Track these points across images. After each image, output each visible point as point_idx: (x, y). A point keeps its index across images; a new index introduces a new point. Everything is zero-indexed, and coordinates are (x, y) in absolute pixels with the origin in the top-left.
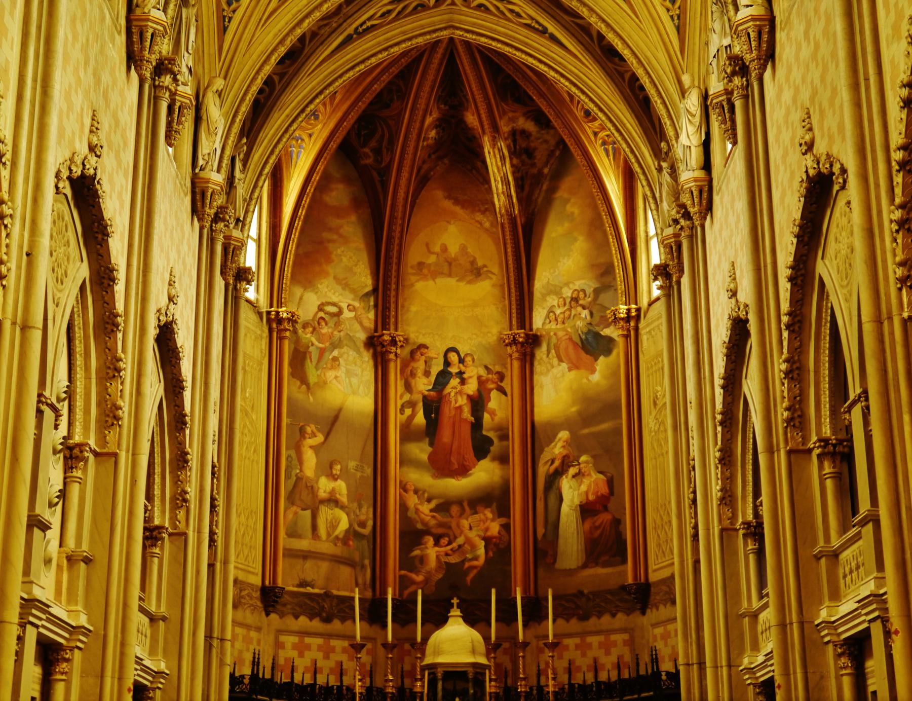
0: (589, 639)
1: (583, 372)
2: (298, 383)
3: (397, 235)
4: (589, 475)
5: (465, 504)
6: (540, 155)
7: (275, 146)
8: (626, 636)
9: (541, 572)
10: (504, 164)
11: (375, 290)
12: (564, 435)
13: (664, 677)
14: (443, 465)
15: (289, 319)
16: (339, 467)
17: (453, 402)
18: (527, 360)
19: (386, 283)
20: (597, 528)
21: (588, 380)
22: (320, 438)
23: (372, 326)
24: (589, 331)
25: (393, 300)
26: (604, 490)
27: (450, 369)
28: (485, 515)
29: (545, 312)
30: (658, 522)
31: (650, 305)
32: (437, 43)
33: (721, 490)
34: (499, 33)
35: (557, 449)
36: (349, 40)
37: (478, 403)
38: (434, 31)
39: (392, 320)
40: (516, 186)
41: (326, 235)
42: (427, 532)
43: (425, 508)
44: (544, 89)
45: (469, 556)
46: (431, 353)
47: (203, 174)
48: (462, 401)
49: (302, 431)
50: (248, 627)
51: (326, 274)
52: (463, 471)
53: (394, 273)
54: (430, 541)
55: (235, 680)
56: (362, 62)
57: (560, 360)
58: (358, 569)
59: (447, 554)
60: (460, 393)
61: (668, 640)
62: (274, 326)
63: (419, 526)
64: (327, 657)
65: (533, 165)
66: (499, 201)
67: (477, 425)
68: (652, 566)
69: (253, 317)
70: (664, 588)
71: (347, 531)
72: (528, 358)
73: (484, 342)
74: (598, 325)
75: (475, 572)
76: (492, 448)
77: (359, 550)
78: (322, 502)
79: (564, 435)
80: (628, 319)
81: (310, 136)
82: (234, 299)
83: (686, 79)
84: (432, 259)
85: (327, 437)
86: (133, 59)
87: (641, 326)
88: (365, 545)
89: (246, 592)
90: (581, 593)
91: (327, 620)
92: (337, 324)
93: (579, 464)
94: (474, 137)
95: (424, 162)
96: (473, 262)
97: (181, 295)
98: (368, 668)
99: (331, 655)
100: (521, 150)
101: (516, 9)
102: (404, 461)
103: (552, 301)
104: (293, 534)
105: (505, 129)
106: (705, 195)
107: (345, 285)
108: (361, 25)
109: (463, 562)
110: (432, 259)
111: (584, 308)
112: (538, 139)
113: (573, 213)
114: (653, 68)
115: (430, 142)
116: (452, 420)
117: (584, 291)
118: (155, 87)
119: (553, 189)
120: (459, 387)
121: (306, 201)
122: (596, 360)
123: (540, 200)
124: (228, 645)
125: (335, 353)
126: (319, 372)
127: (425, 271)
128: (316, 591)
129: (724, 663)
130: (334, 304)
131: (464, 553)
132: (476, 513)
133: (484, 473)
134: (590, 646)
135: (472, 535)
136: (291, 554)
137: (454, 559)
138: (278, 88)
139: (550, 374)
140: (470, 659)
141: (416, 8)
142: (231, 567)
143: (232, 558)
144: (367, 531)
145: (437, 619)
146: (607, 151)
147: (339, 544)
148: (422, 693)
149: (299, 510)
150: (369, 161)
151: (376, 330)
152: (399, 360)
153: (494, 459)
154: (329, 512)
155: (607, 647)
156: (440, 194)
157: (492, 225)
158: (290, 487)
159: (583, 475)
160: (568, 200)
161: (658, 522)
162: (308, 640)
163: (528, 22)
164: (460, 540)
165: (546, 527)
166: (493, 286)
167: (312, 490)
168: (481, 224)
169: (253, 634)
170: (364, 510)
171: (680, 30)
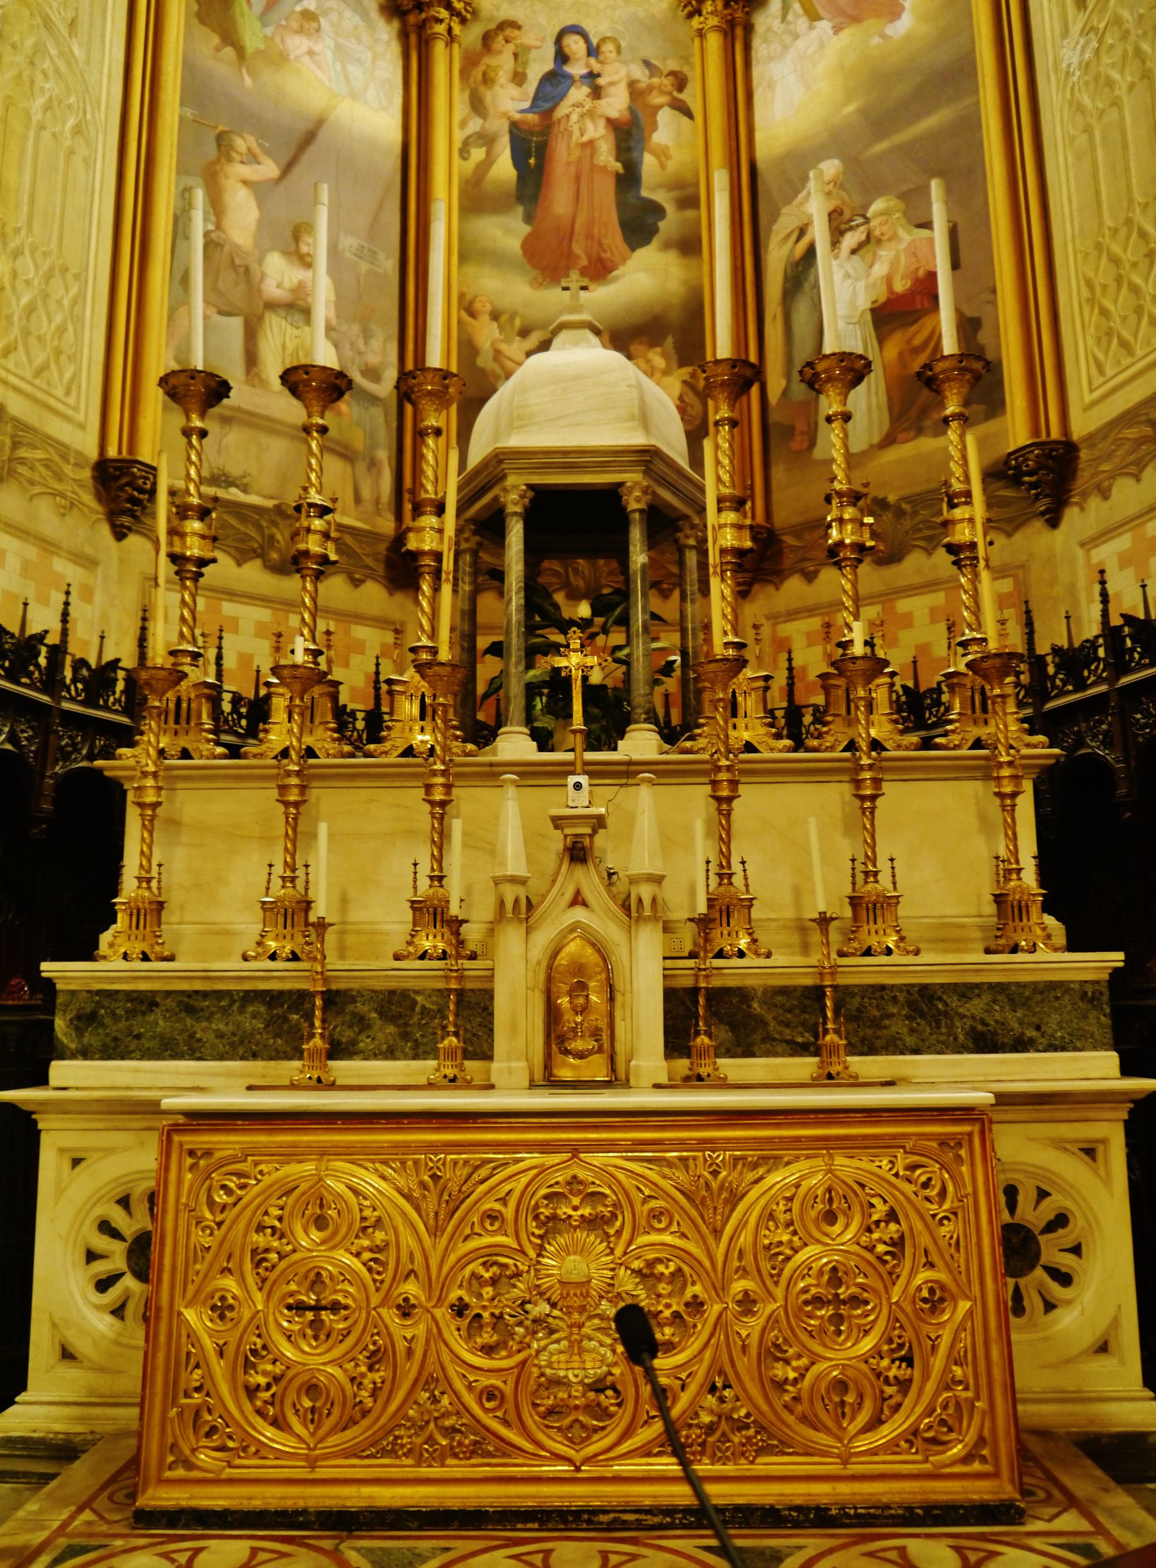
0: (904, 605)
1: (870, 24)
2: (216, 40)
4: (894, 237)
9: (779, 473)
12: (831, 167)
17: (576, 134)
20: (916, 351)
21: (883, 36)
22: (269, 169)
28: (648, 361)
37: (629, 135)
46: (527, 37)
48: (597, 131)
49: (222, 140)
52: (600, 270)
57: (813, 16)
58: (361, 466)
60: (591, 114)
67: (629, 178)
68: (1074, 411)
70: (1131, 433)
72: (739, 32)
73: (641, 14)
76: (662, 225)
78: (271, 306)
89: (39, 454)
93: (867, 220)
116: (573, 170)
120: (588, 104)
126: (269, 31)
128: (254, 499)
139: (791, 54)
140: (638, 439)
148: (438, 556)
152: (456, 47)
153: (667, 246)
154: (291, 331)
159: (879, 242)
161: (1104, 274)
165: (788, 376)
167: (247, 275)
170: (376, 343)
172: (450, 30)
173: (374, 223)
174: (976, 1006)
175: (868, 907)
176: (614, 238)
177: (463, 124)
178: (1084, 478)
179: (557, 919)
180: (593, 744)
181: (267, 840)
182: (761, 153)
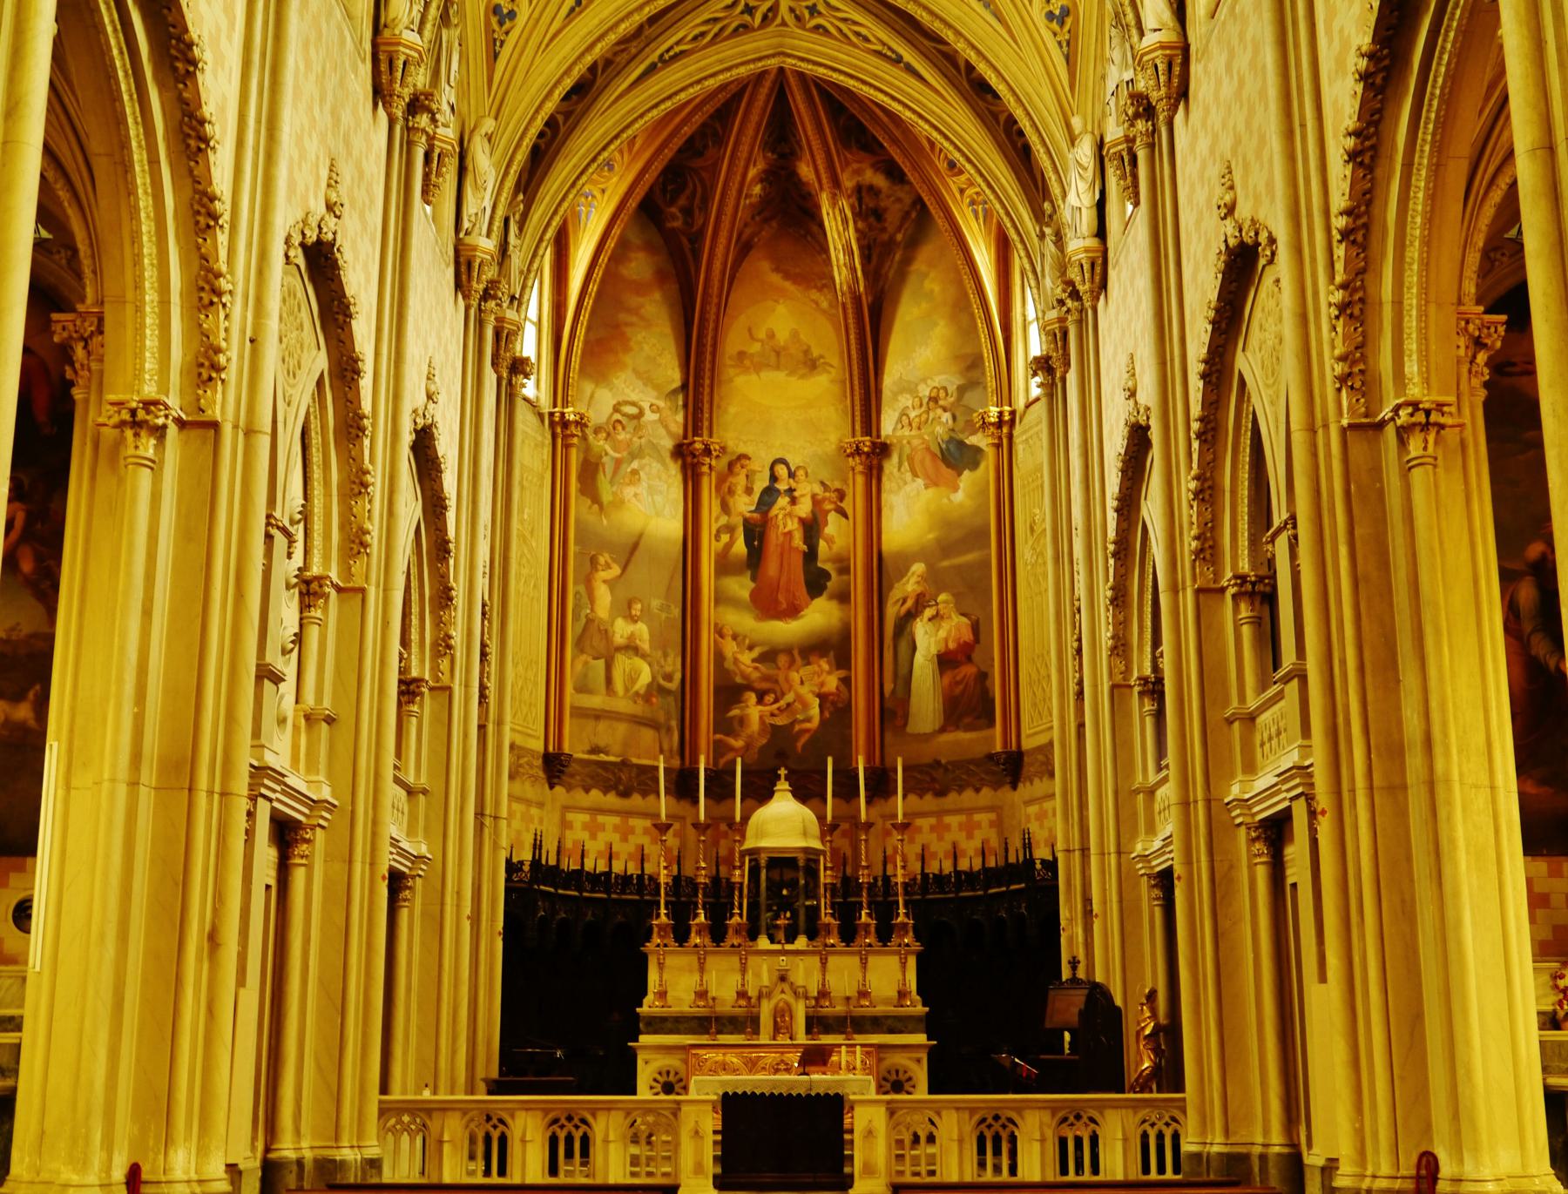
0: (948, 819)
3: (712, 317)
5: (796, 653)
6: (892, 218)
7: (560, 204)
8: (992, 816)
10: (846, 228)
11: (684, 386)
12: (918, 568)
13: (1038, 866)
14: (769, 604)
15: (577, 423)
16: (639, 606)
18: (874, 474)
19: (699, 376)
20: (958, 683)
22: (616, 570)
23: (681, 431)
24: (951, 440)
25: (706, 398)
26: (967, 636)
27: (777, 486)
29: (897, 415)
30: (1034, 676)
31: (1028, 406)
32: (762, 75)
33: (1113, 638)
34: (841, 62)
35: (909, 585)
36: (652, 69)
37: (811, 528)
38: (760, 59)
39: (706, 424)
40: (862, 256)
41: (623, 317)
42: (749, 688)
43: (746, 658)
44: (897, 133)
45: (800, 717)
46: (754, 465)
47: (468, 240)
48: (793, 525)
49: (593, 561)
50: (528, 802)
51: (623, 367)
52: (793, 612)
53: (708, 365)
54: (752, 697)
55: (512, 867)
56: (669, 97)
58: (663, 731)
59: (772, 715)
60: (790, 515)
61: (1044, 820)
62: (559, 430)
63: (738, 680)
64: (625, 839)
65: (884, 230)
66: (841, 276)
67: (811, 555)
68: (1025, 731)
69: (534, 420)
70: (1041, 757)
71: (650, 686)
72: (875, 472)
74: (962, 431)
75: (806, 737)
77: (665, 709)
78: (618, 649)
79: (918, 568)
80: (1000, 424)
81: (603, 191)
82: (508, 396)
83: (1076, 122)
84: (755, 348)
85: (624, 569)
86: (380, 93)
87: (1015, 433)
88: (672, 703)
90: (938, 763)
91: (625, 794)
92: (637, 429)
94: (810, 194)
95: (746, 225)
96: (807, 352)
97: (443, 392)
98: (675, 853)
99: (630, 837)
100: (868, 211)
101: (863, 31)
102: (720, 599)
103: (906, 401)
104: (582, 688)
105: (848, 183)
106: (1098, 270)
107: (647, 379)
108: (668, 51)
109: (792, 724)
110: (755, 348)
111: (945, 410)
112: (888, 197)
113: (932, 291)
114: (1035, 108)
115: (754, 200)
117: (945, 389)
118: (409, 129)
119: (907, 261)
120: (789, 508)
121: (598, 274)
122: (960, 474)
123: (891, 274)
124: (503, 824)
125: (635, 465)
127: (747, 362)
128: (612, 759)
129: (1113, 849)
130: (634, 404)
131: (795, 713)
132: (809, 663)
133: (819, 615)
134: (948, 828)
135: (805, 691)
136: (581, 713)
137: (781, 721)
138: (563, 130)
139: (902, 493)
140: (802, 844)
141: (736, 30)
142: (507, 729)
143: (508, 717)
144: (674, 685)
145: (760, 793)
146: (976, 213)
147: (640, 701)
149: (590, 659)
150: (677, 224)
151: (685, 437)
153: (831, 597)
154: (628, 661)
155: (969, 829)
156: (765, 266)
157: (831, 305)
158: (579, 630)
160: (925, 276)
161: (1034, 676)
162: (601, 819)
163: (879, 47)
164: (789, 698)
166: (832, 381)
167: (606, 634)
168: (817, 303)
169: (534, 811)
170: (670, 660)
171: (1068, 59)
172: (710, 467)
173: (669, 588)
174: (889, 1022)
175: (863, 994)
176: (802, 591)
177: (717, 519)
178: (1025, 772)
179: (778, 997)
180: (788, 942)
181: (691, 971)
182: (885, 547)
